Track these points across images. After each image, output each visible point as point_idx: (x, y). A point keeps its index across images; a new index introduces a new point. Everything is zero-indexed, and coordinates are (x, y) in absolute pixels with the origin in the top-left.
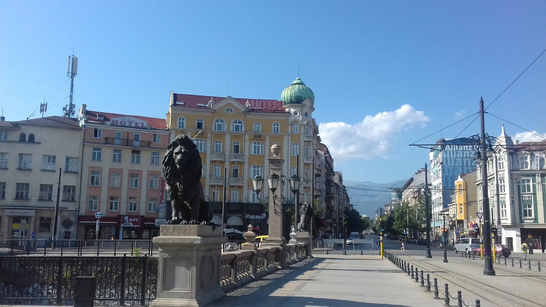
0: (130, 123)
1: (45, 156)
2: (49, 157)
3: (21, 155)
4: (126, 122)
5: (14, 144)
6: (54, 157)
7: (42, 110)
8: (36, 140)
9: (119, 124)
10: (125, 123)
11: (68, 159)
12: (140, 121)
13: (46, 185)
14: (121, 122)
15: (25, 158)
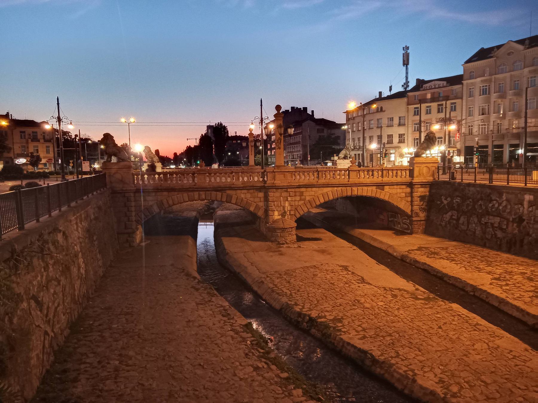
0: (435, 85)
1: (388, 118)
2: (391, 118)
3: (378, 120)
4: (432, 85)
5: (374, 114)
6: (393, 118)
7: (390, 90)
8: (383, 110)
9: (428, 88)
10: (432, 86)
11: (400, 118)
12: (441, 82)
13: (390, 135)
14: (429, 87)
15: (380, 121)
